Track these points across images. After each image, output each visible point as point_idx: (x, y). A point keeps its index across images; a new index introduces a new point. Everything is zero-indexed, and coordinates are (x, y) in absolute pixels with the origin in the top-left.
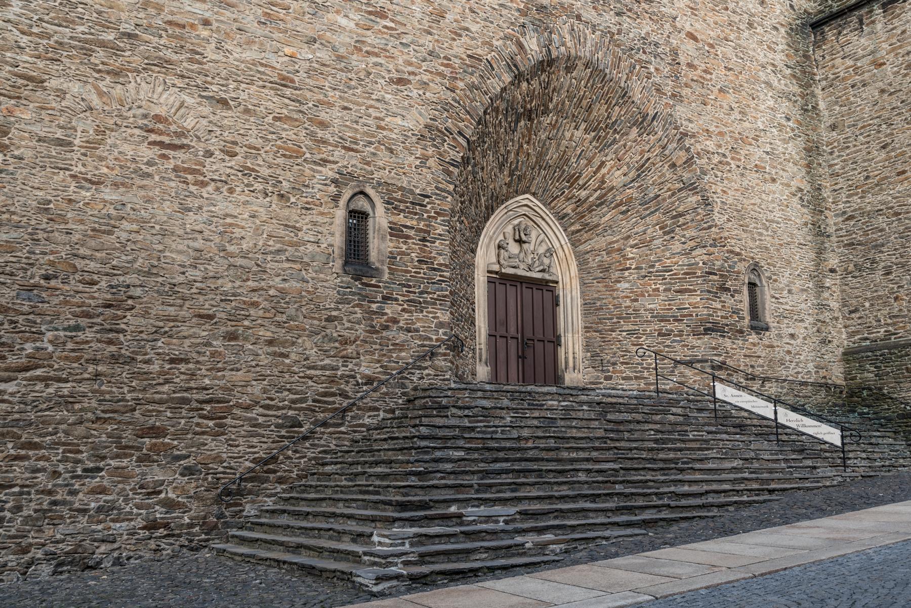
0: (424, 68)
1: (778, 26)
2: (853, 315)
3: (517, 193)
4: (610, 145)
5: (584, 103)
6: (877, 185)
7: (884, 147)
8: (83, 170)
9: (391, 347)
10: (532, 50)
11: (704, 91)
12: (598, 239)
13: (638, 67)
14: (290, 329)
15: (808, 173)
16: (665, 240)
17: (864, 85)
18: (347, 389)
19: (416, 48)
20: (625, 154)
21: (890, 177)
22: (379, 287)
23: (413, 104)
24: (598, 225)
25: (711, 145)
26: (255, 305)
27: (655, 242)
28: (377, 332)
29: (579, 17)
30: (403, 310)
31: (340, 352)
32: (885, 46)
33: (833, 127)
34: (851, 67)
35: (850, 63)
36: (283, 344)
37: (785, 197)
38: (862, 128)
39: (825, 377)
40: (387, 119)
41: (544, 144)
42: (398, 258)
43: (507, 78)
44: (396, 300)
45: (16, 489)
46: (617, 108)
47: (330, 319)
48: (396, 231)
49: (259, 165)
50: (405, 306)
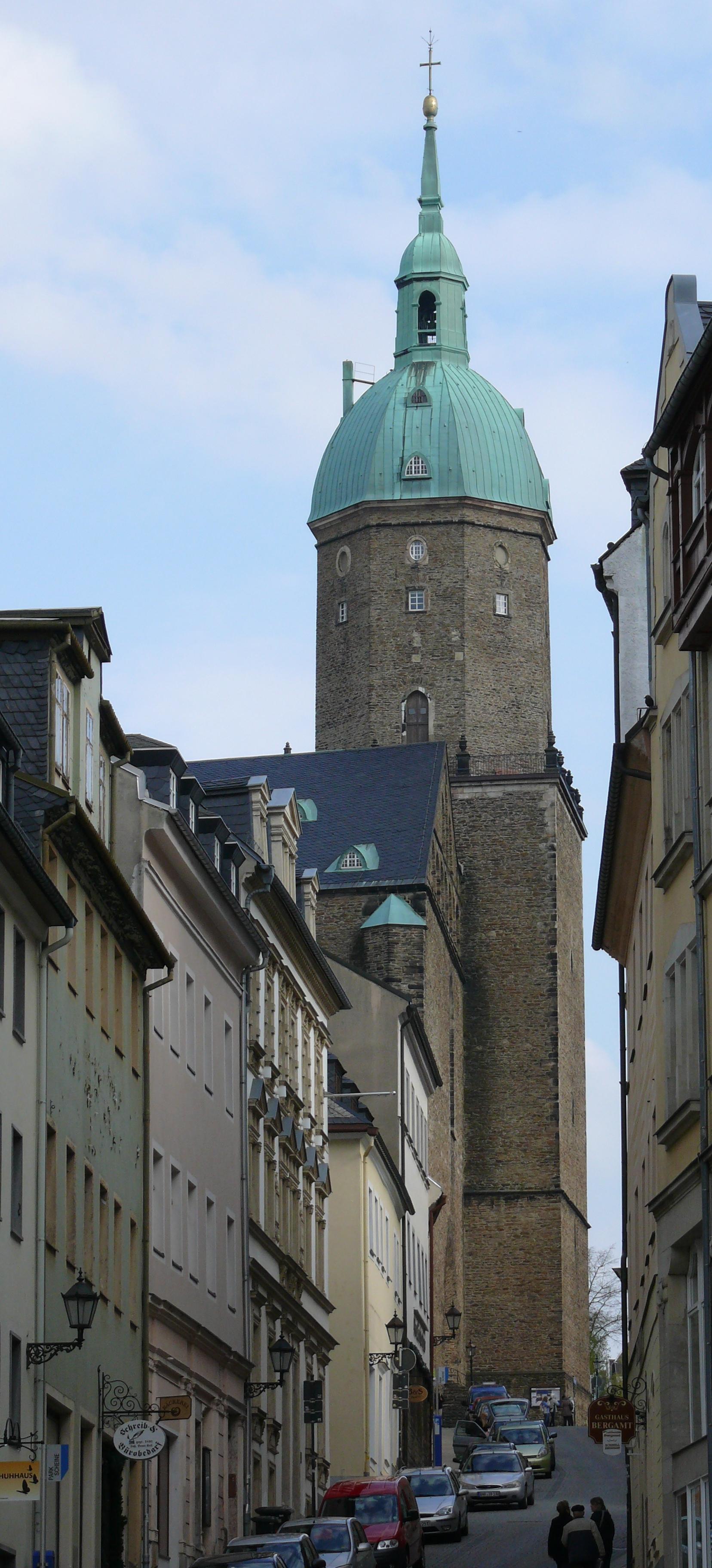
7: (498, 1273)
17: (490, 1237)
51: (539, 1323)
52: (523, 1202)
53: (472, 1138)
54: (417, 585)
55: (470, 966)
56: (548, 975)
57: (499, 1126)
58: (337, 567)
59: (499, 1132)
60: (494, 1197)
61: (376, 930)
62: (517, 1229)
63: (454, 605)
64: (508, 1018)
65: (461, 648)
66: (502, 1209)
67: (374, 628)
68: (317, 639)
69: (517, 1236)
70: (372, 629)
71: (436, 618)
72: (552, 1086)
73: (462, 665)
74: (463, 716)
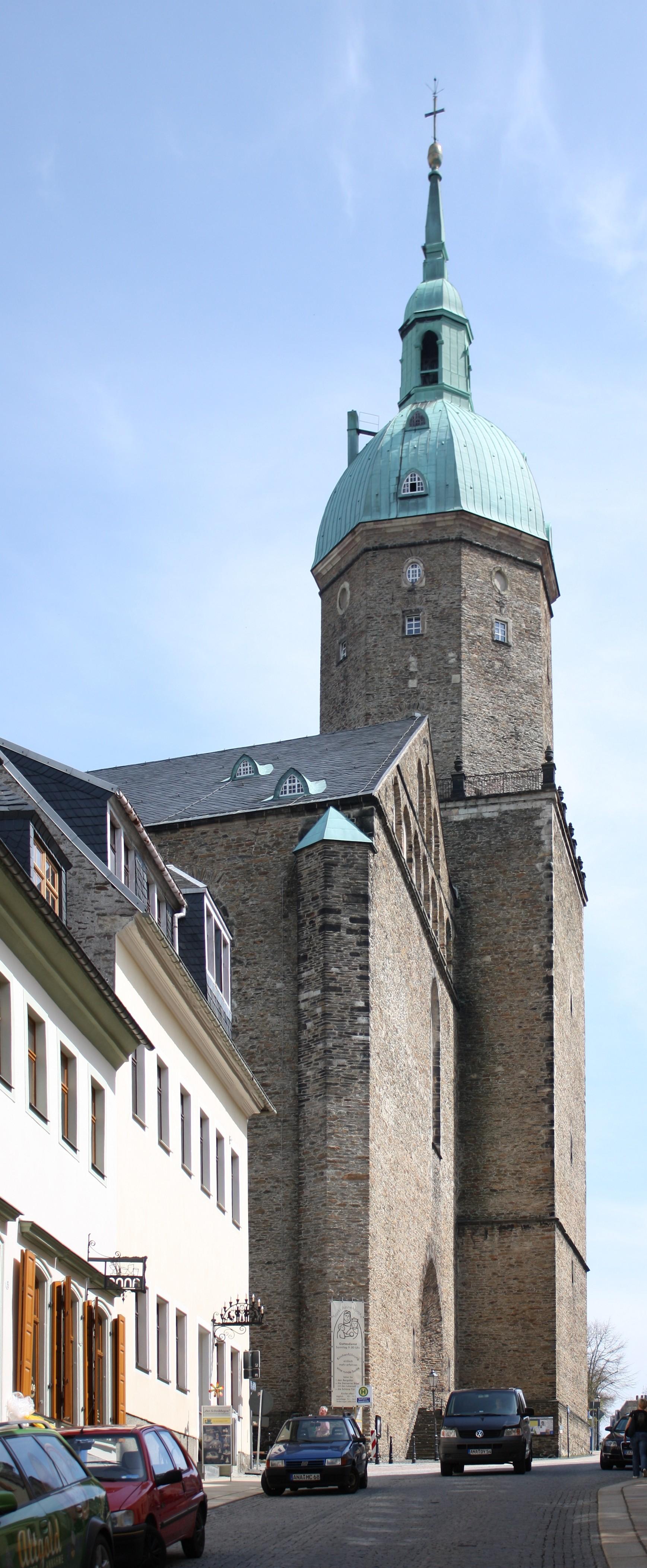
17: (484, 1267)
51: (533, 1352)
52: (518, 1231)
53: (466, 1167)
54: (413, 608)
55: (464, 993)
56: (544, 998)
57: (493, 1155)
58: (338, 606)
59: (493, 1161)
60: (489, 1227)
61: (311, 851)
62: (510, 1259)
63: (451, 626)
64: (502, 1045)
65: (458, 670)
67: (371, 655)
68: (321, 685)
70: (368, 656)
71: (433, 641)
72: (547, 1112)
73: (458, 688)
74: (460, 740)
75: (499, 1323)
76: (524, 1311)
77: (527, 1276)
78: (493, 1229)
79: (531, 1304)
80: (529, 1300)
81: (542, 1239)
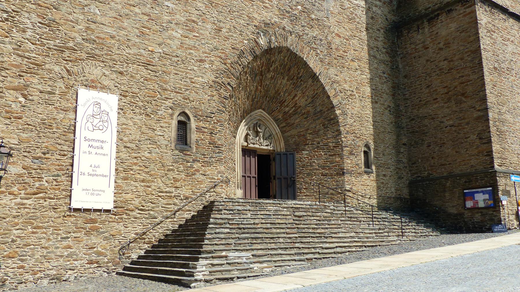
0: (212, 54)
1: (380, 29)
2: (413, 165)
3: (256, 109)
4: (299, 87)
5: (287, 67)
6: (424, 105)
7: (428, 87)
8: (60, 105)
9: (196, 183)
10: (262, 44)
11: (344, 61)
12: (294, 130)
13: (312, 51)
14: (151, 175)
15: (393, 98)
16: (325, 131)
17: (419, 57)
18: (177, 201)
19: (208, 45)
20: (306, 91)
21: (430, 101)
22: (191, 155)
23: (207, 70)
24: (294, 124)
25: (347, 86)
26: (136, 164)
27: (320, 132)
28: (190, 176)
29: (284, 29)
30: (202, 166)
31: (174, 185)
32: (429, 39)
33: (405, 77)
34: (414, 48)
35: (413, 46)
36: (148, 181)
37: (382, 110)
38: (418, 77)
39: (400, 195)
40: (195, 78)
41: (268, 86)
42: (200, 142)
43: (250, 58)
44: (199, 161)
45: (32, 246)
46: (302, 69)
47: (169, 170)
48: (199, 129)
49: (137, 101)
50: (203, 164)
52: (443, 17)
62: (439, 43)
66: (426, 30)
69: (441, 49)
75: (435, 103)
76: (456, 87)
77: (455, 54)
78: (423, 23)
79: (461, 79)
80: (459, 75)
81: (465, 16)
